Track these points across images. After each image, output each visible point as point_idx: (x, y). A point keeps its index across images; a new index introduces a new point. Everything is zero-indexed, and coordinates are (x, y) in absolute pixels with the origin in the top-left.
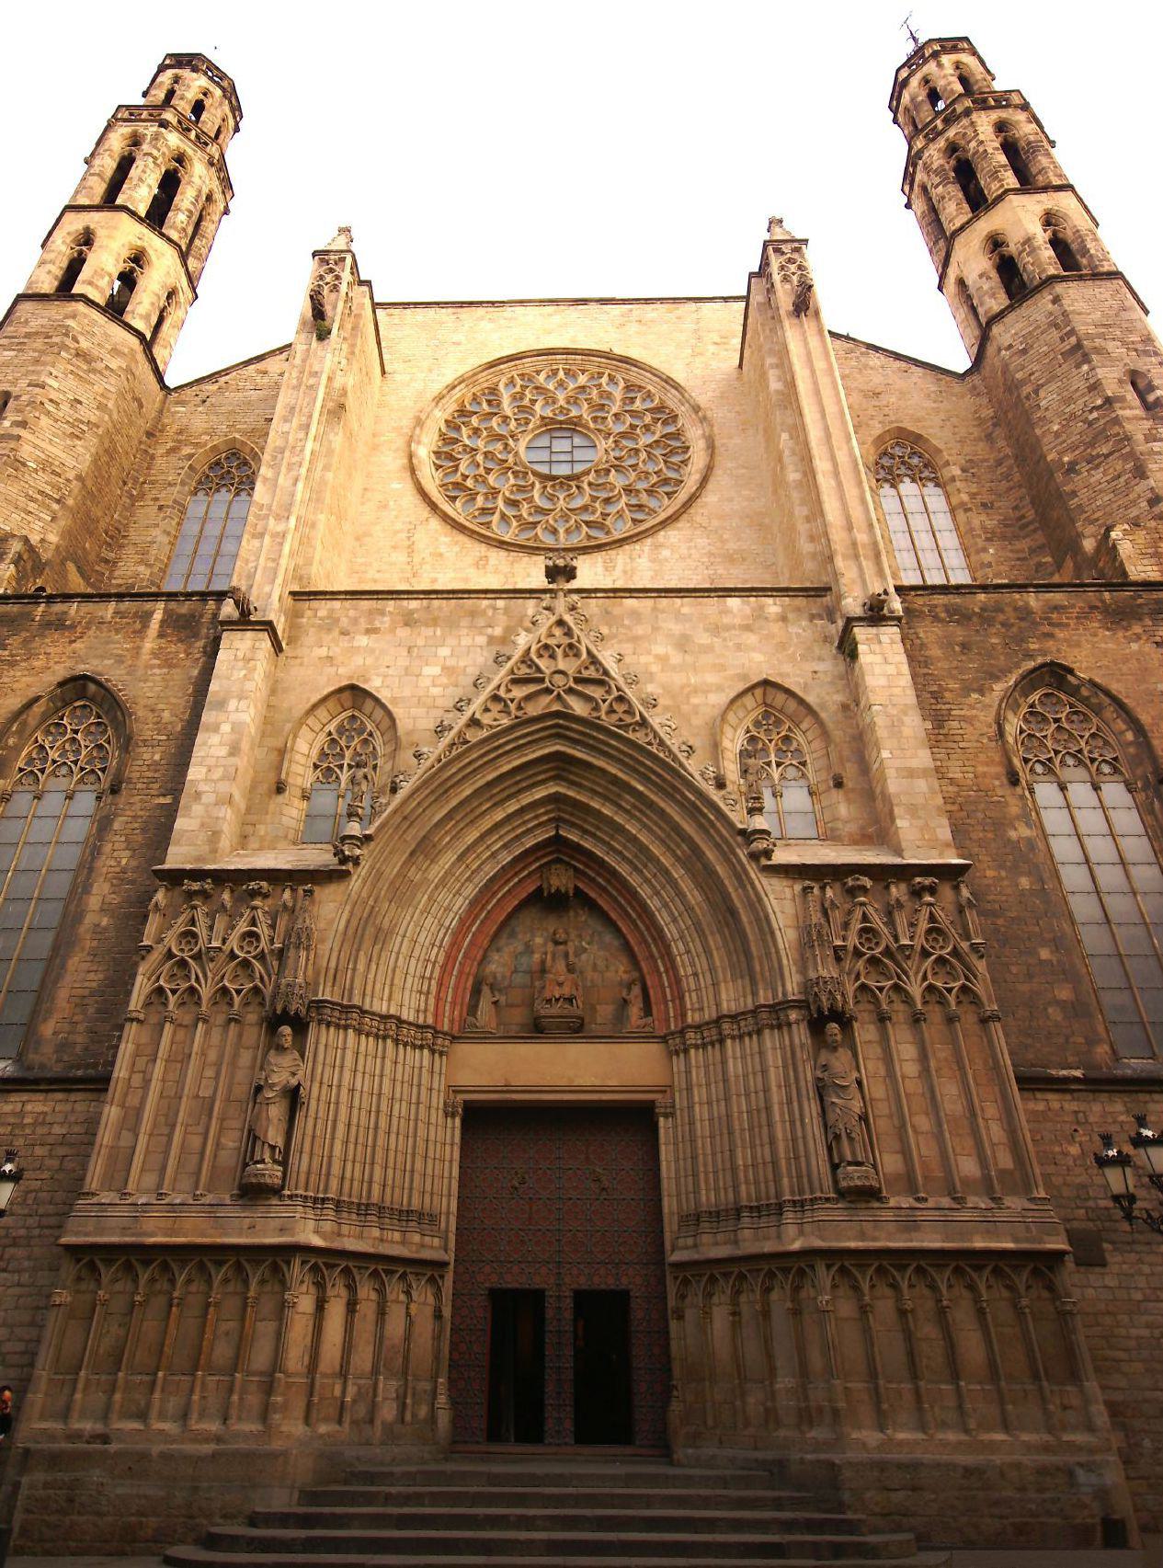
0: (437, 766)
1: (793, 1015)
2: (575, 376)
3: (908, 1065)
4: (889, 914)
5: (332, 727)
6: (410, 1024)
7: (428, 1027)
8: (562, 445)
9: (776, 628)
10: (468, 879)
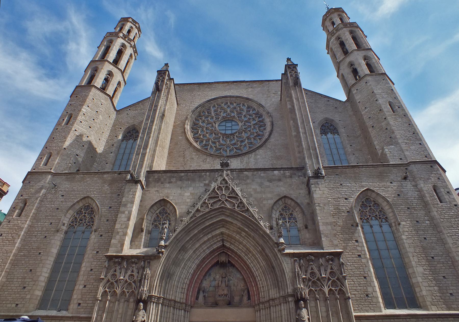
0: (187, 224)
1: (290, 299)
2: (233, 104)
4: (319, 268)
5: (158, 212)
6: (178, 302)
7: (184, 303)
8: (229, 124)
10: (197, 258)
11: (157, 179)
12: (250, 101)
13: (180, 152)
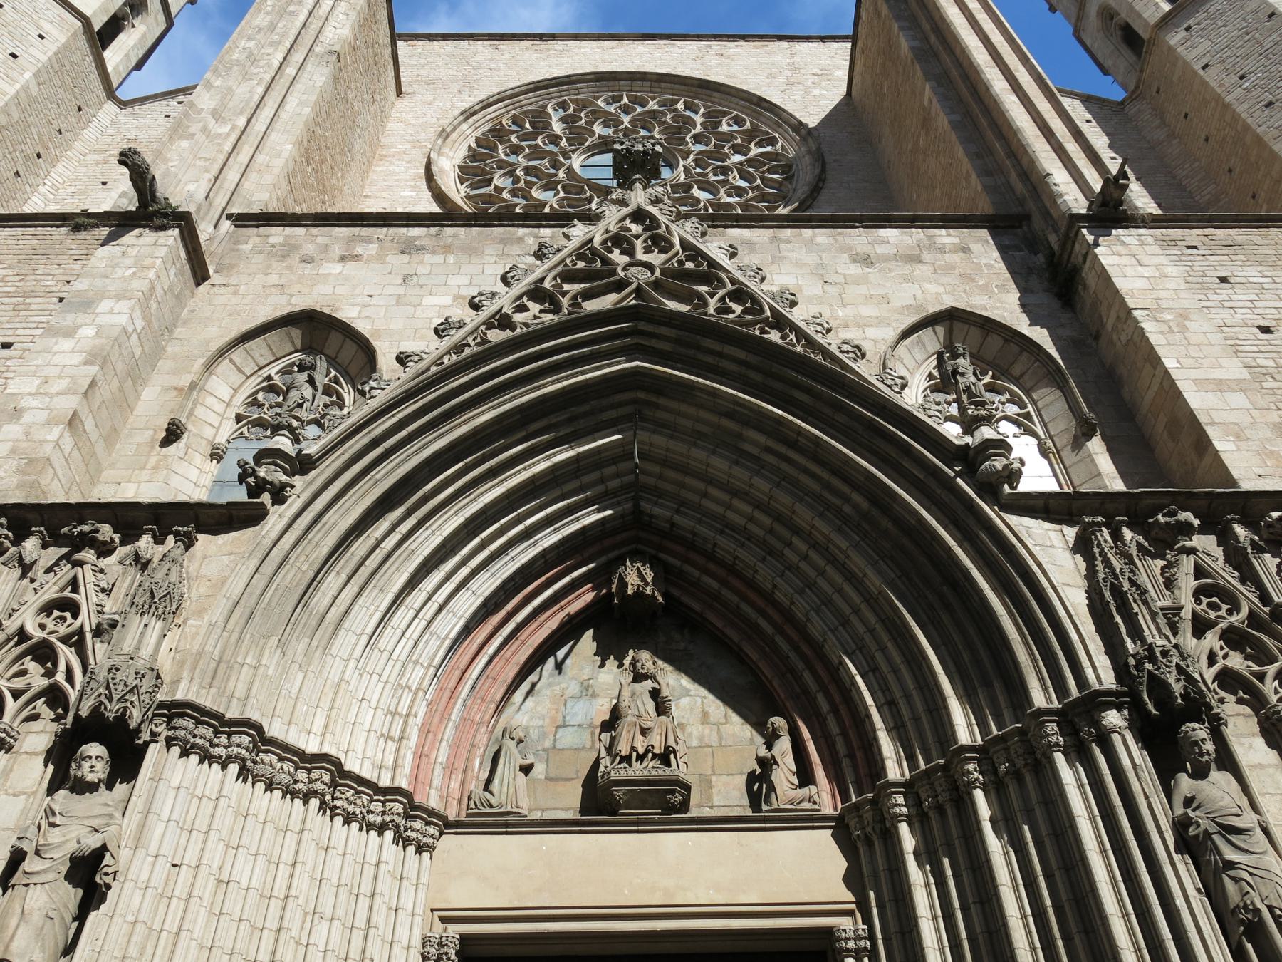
0: (434, 369)
6: (361, 781)
9: (956, 258)
11: (283, 245)
12: (715, 94)
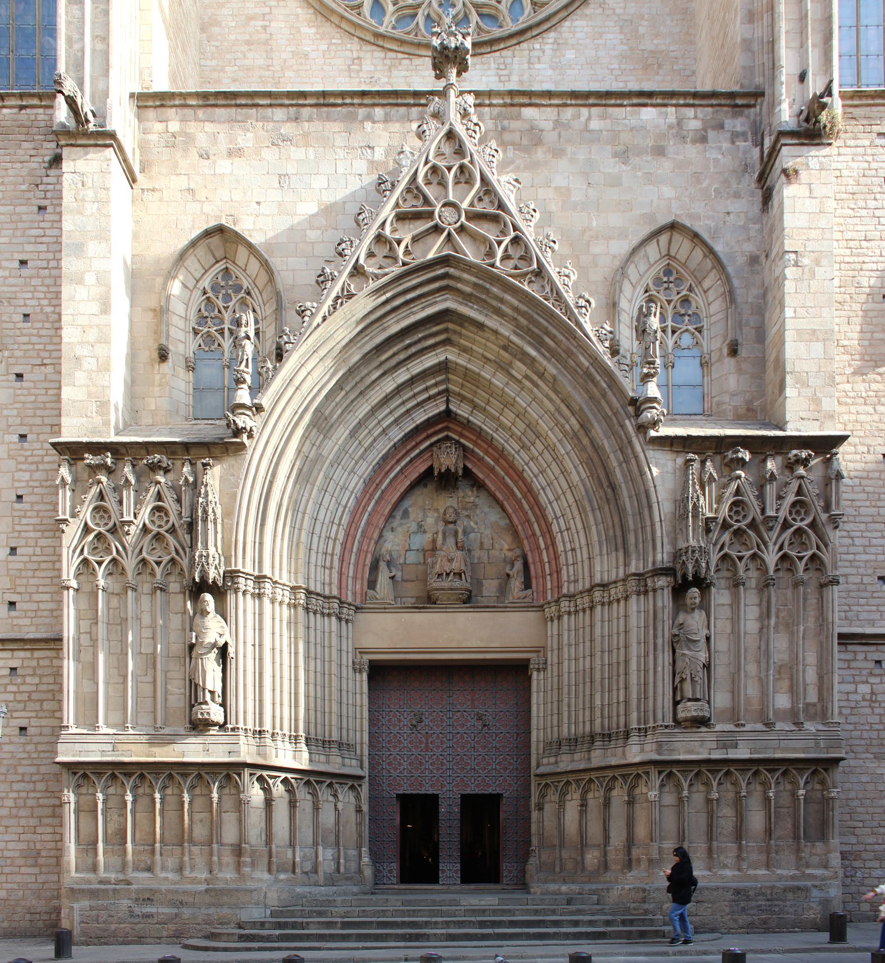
3: (750, 624)
4: (761, 488)
13: (250, 18)
